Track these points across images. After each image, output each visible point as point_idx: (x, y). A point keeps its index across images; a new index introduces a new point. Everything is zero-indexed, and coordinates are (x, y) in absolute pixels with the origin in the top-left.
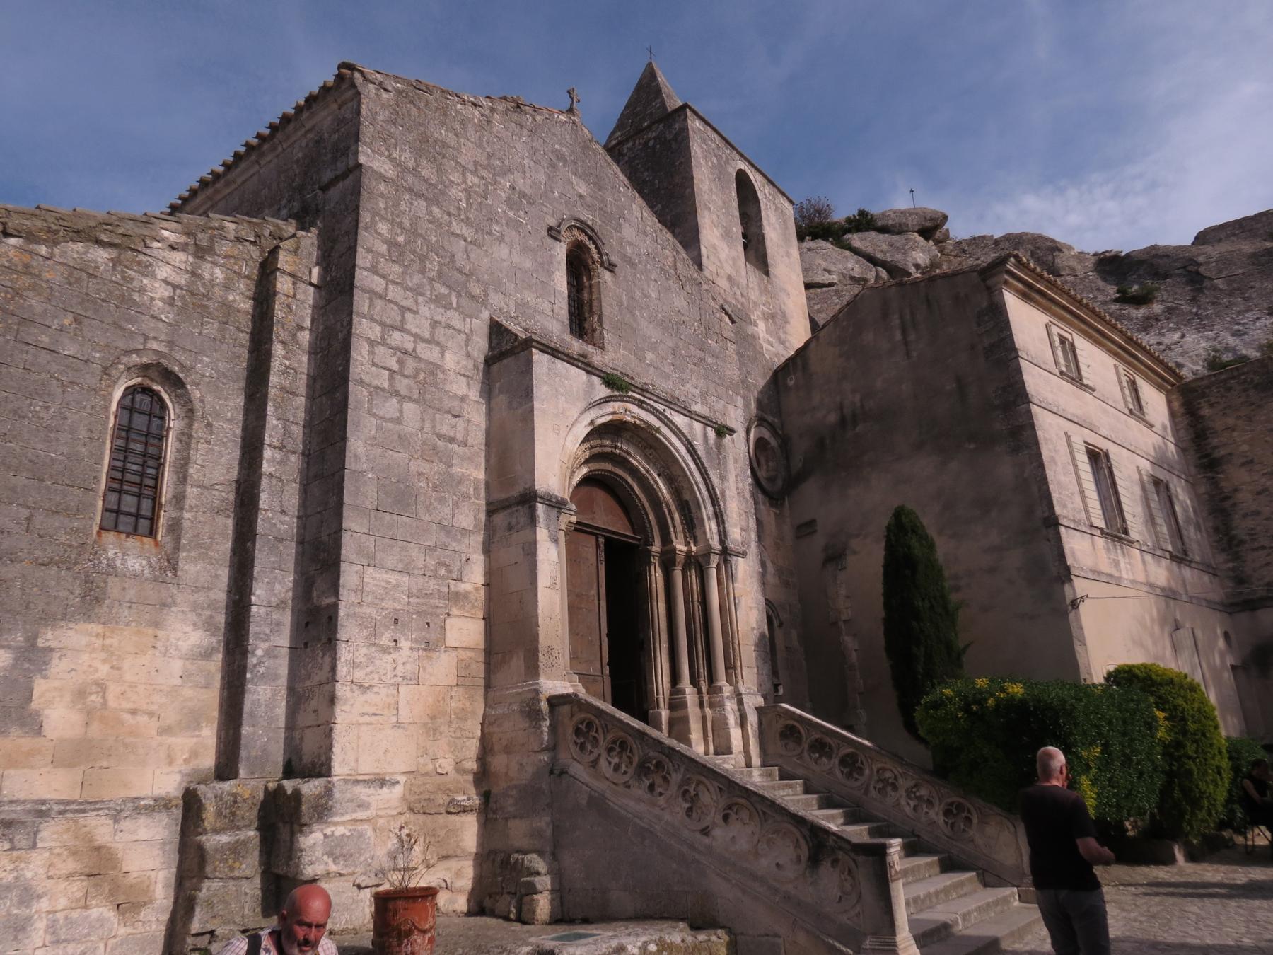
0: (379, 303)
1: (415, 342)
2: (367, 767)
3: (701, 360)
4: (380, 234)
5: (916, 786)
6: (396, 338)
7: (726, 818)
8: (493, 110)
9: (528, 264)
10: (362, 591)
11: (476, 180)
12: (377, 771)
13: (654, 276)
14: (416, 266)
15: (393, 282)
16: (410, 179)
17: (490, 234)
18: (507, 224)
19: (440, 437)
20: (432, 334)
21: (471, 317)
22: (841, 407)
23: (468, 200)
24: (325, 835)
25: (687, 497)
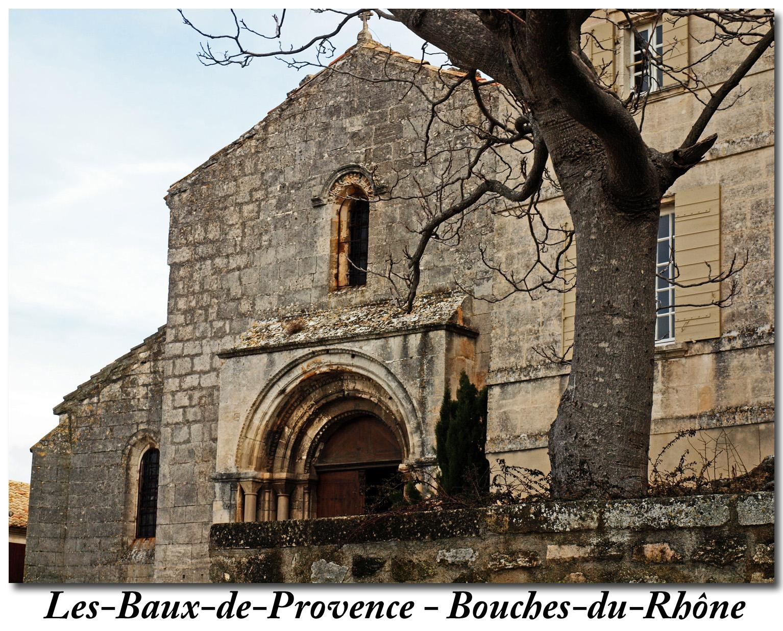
0: (178, 361)
6: (191, 381)
9: (292, 251)
10: (166, 561)
11: (251, 207)
14: (203, 318)
20: (211, 366)
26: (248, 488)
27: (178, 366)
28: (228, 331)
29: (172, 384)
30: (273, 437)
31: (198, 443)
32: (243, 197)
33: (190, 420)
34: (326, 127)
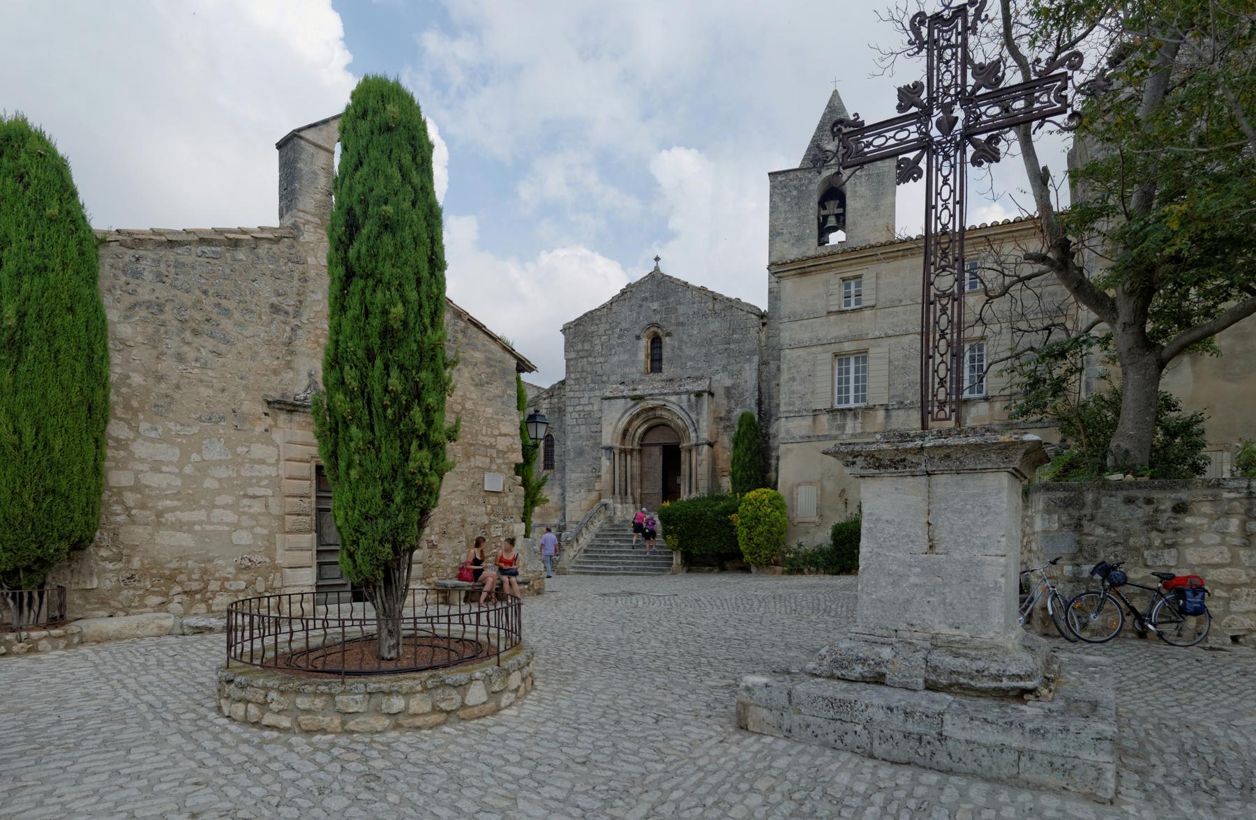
6: (578, 408)
9: (626, 357)
26: (617, 452)
29: (570, 409)
30: (625, 432)
32: (601, 332)
34: (641, 306)
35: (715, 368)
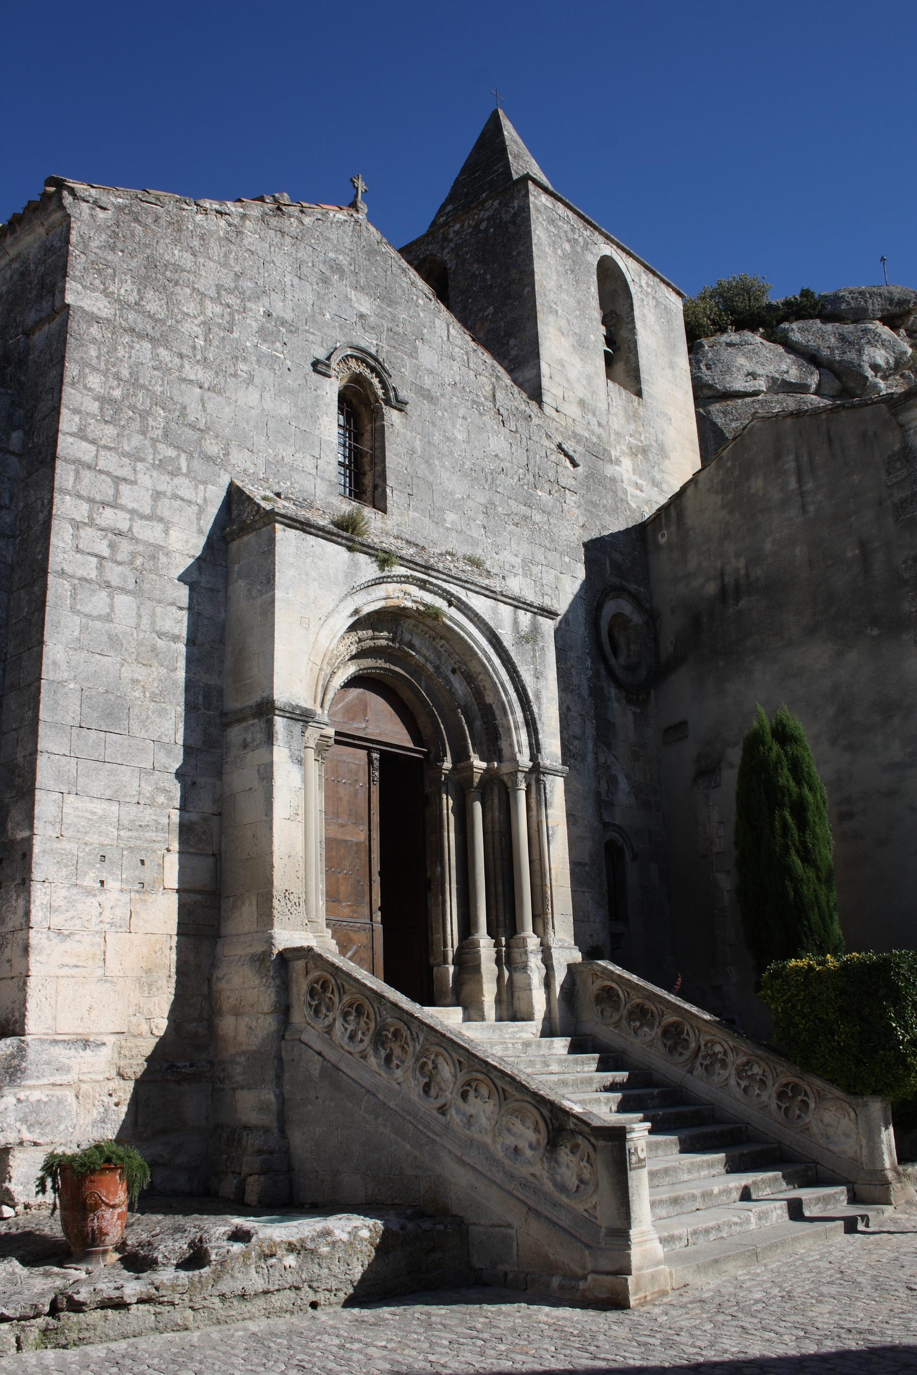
0: (87, 475)
1: (131, 520)
2: (69, 1025)
3: (525, 518)
4: (90, 389)
5: (747, 1063)
6: (108, 517)
7: (464, 1096)
8: (244, 217)
9: (285, 410)
11: (218, 309)
12: (80, 1030)
13: (462, 412)
14: (136, 426)
15: (106, 447)
16: (131, 316)
17: (235, 375)
18: (258, 361)
19: (160, 635)
20: (154, 508)
21: (204, 483)
22: (722, 574)
23: (206, 335)
24: (19, 1100)
25: (489, 699)
27: (86, 481)
28: (184, 470)
31: (128, 629)
33: (113, 584)
35: (506, 556)
